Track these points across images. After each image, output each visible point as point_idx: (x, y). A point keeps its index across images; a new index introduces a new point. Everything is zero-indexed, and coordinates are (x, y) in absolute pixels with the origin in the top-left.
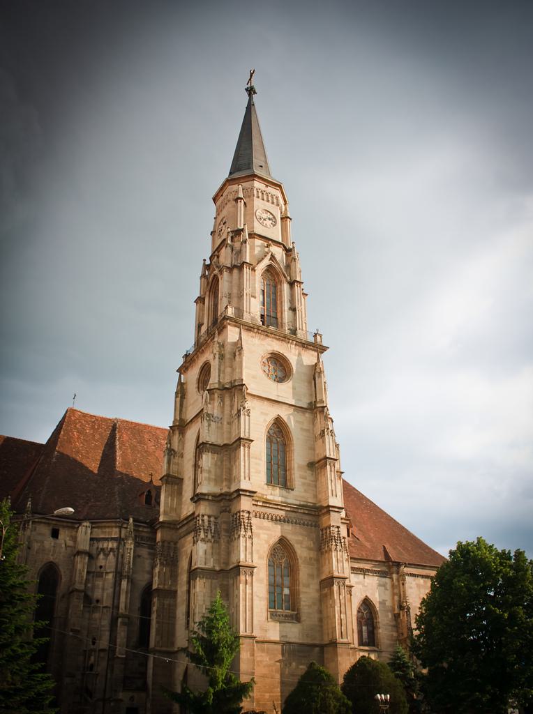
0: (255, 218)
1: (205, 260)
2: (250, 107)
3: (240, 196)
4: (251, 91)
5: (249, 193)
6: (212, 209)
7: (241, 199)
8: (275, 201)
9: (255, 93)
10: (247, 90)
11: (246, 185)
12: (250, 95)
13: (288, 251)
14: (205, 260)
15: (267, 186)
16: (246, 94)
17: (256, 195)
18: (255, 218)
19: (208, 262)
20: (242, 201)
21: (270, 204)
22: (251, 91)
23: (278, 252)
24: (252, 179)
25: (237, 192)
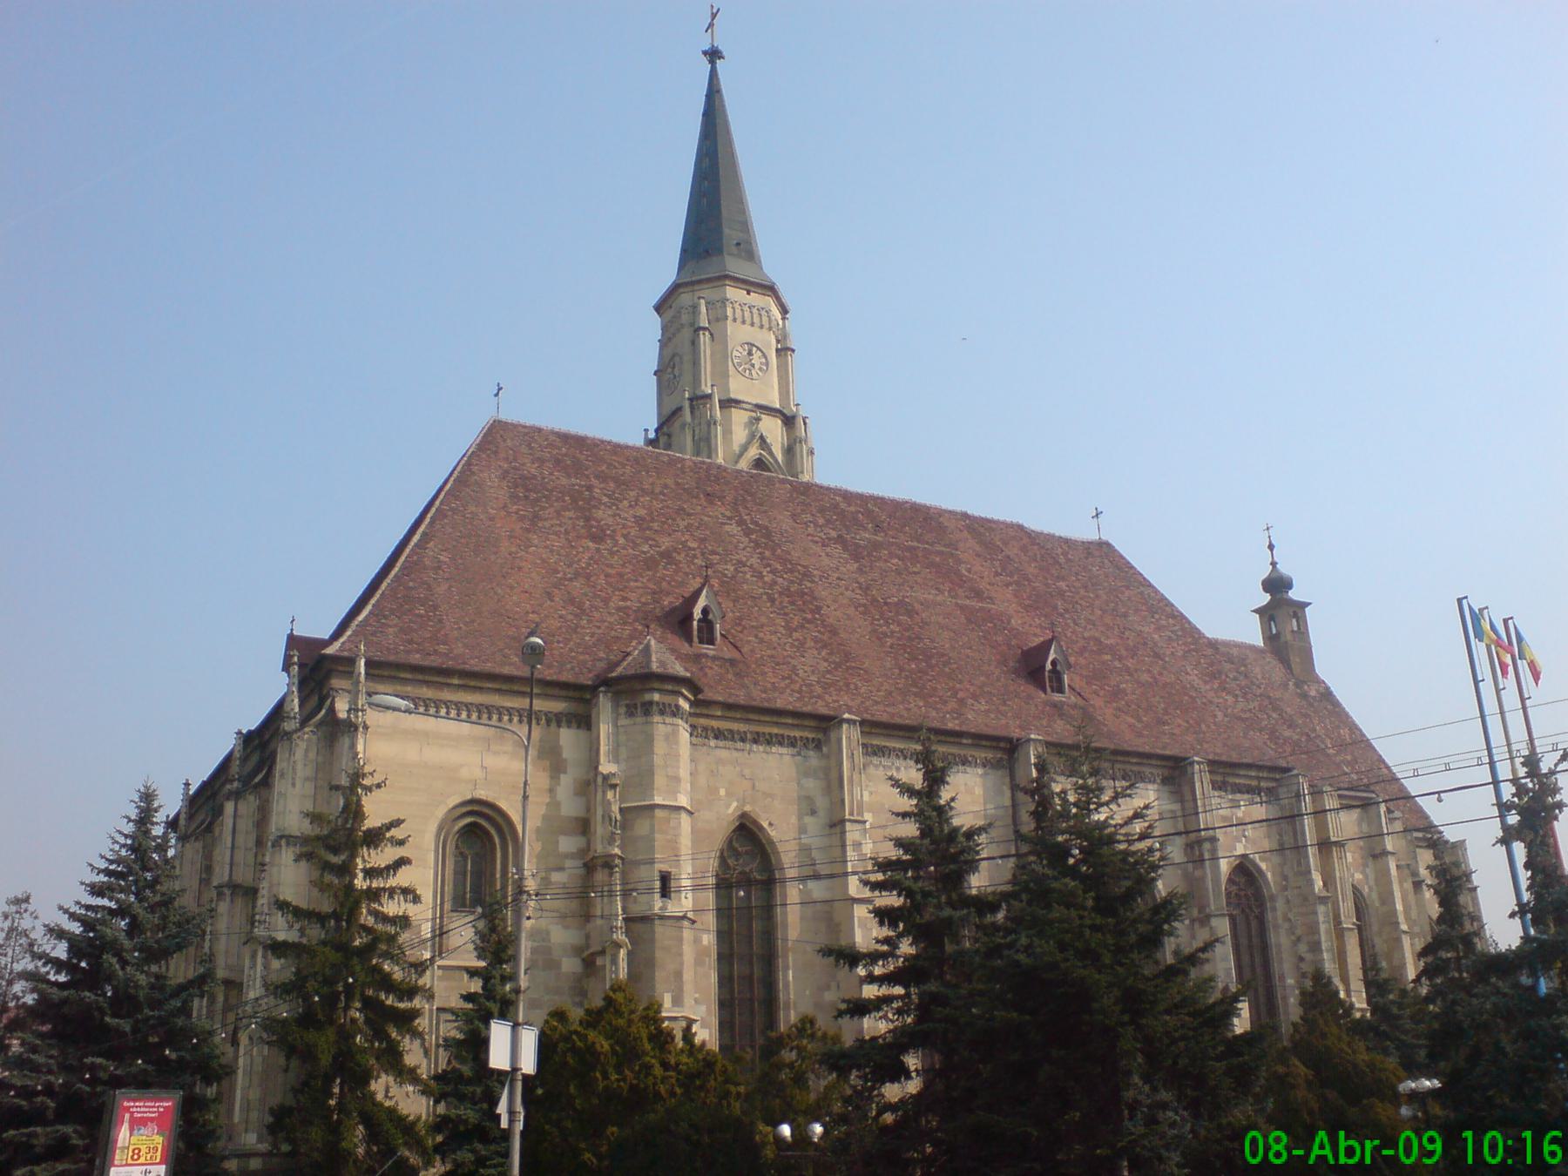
0: (730, 363)
1: (646, 430)
2: (713, 93)
3: (702, 325)
4: (713, 55)
5: (718, 308)
6: (655, 322)
7: (705, 329)
8: (765, 319)
9: (721, 57)
10: (705, 53)
11: (708, 292)
12: (712, 62)
13: (789, 421)
14: (646, 430)
15: (748, 293)
16: (705, 61)
17: (730, 319)
18: (730, 363)
19: (652, 435)
20: (707, 333)
21: (756, 329)
22: (713, 55)
23: (772, 429)
24: (719, 283)
25: (695, 307)
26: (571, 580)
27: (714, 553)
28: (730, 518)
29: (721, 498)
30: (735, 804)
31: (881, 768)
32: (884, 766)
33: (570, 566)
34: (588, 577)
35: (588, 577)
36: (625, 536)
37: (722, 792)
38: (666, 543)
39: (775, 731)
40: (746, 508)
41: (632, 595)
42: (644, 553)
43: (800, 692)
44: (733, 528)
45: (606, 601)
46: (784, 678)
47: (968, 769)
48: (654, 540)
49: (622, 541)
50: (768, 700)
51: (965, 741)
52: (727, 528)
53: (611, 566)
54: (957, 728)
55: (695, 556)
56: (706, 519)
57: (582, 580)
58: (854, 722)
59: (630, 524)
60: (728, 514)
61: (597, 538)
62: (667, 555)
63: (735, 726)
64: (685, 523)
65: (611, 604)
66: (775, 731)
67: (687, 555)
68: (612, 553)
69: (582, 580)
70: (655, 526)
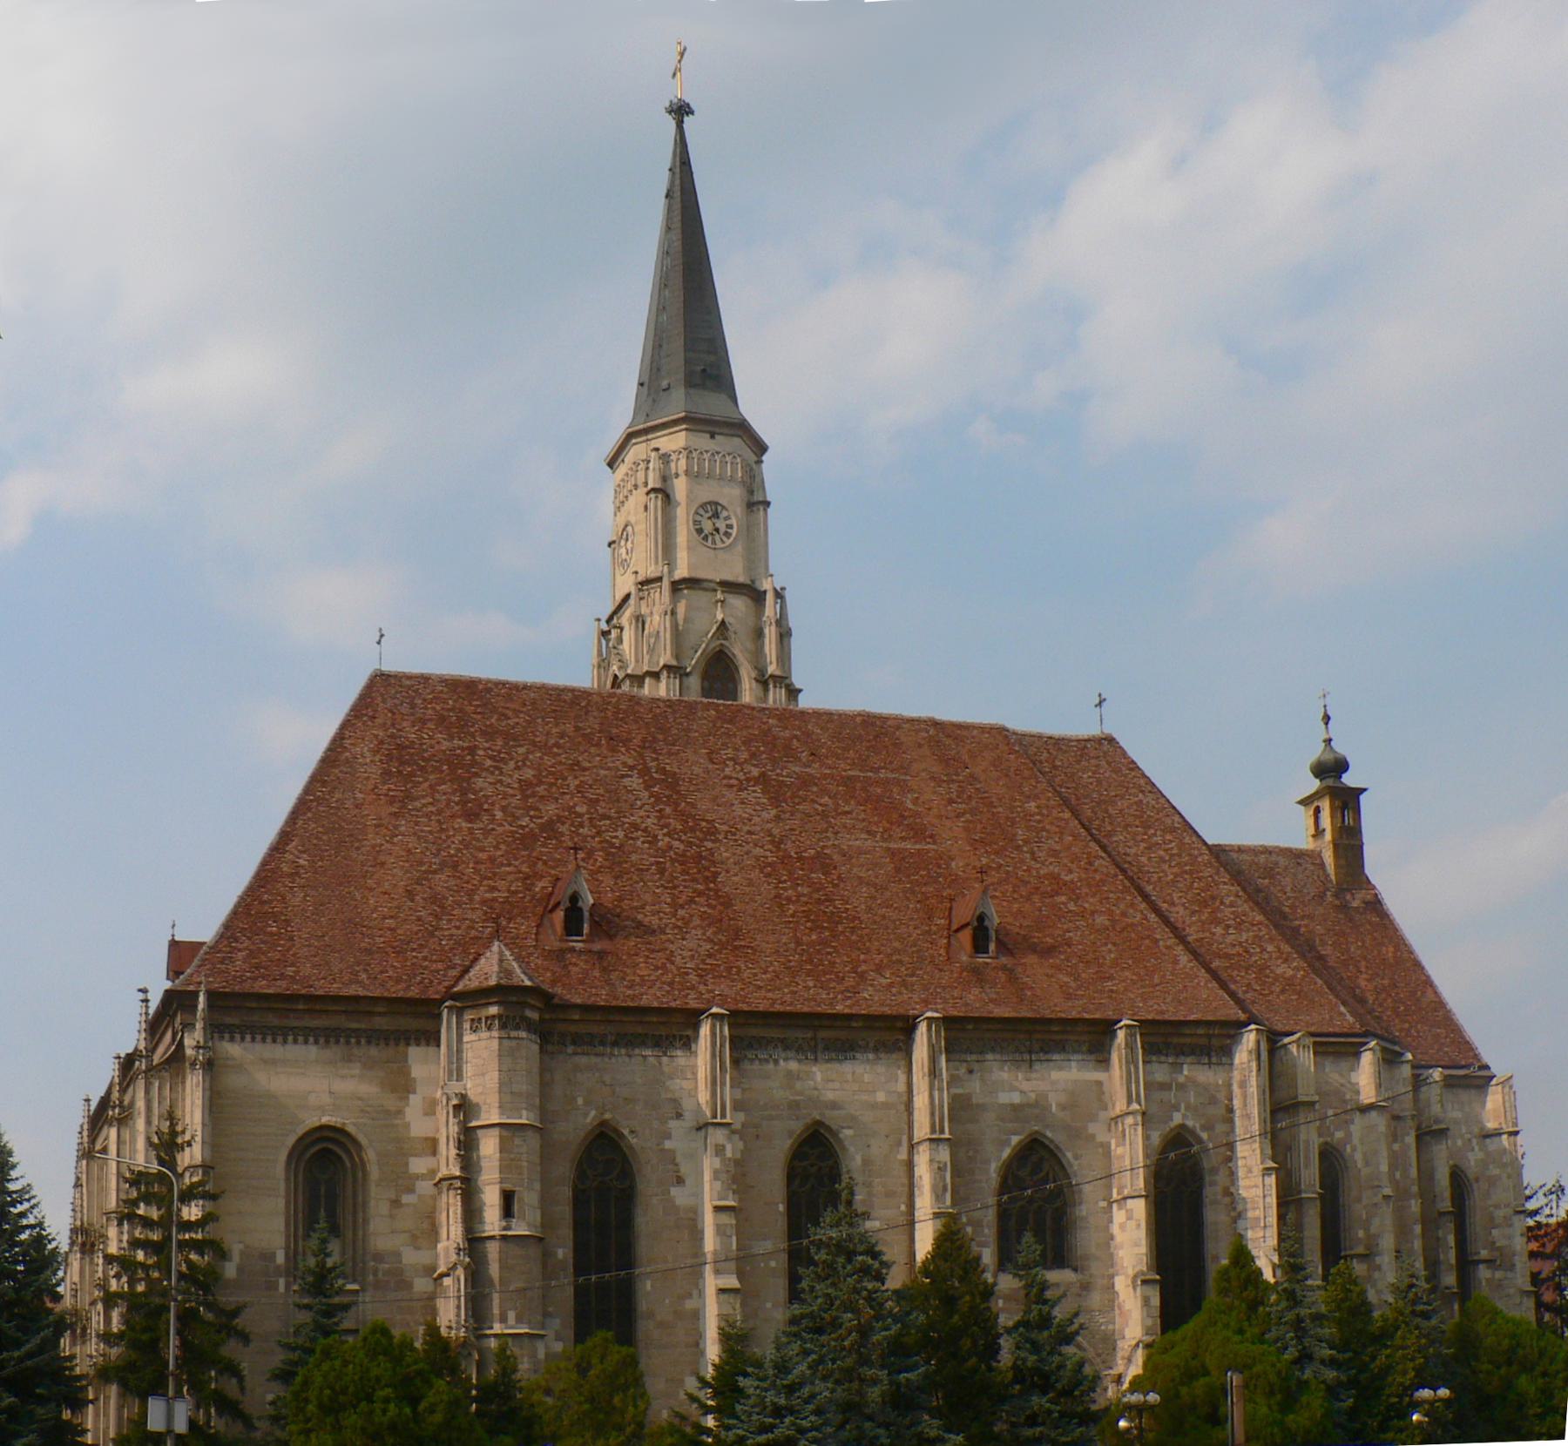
26: (435, 872)
27: (604, 817)
28: (632, 768)
29: (626, 742)
30: (593, 1113)
31: (757, 1062)
32: (760, 1060)
33: (436, 855)
34: (455, 866)
35: (455, 866)
36: (504, 809)
37: (580, 1101)
38: (550, 809)
39: (640, 1030)
40: (655, 751)
41: (502, 884)
42: (522, 827)
43: (671, 984)
44: (634, 782)
45: (471, 894)
46: (657, 968)
47: (858, 1055)
48: (537, 809)
49: (499, 815)
50: (633, 998)
51: (854, 1024)
52: (626, 781)
53: (482, 850)
54: (847, 1011)
55: (581, 825)
56: (603, 772)
57: (448, 872)
58: (722, 1015)
59: (511, 791)
60: (630, 762)
61: (471, 816)
62: (550, 827)
63: (595, 1029)
64: (577, 782)
65: (477, 898)
66: (640, 1030)
67: (572, 825)
68: (487, 832)
69: (448, 872)
70: (541, 790)
